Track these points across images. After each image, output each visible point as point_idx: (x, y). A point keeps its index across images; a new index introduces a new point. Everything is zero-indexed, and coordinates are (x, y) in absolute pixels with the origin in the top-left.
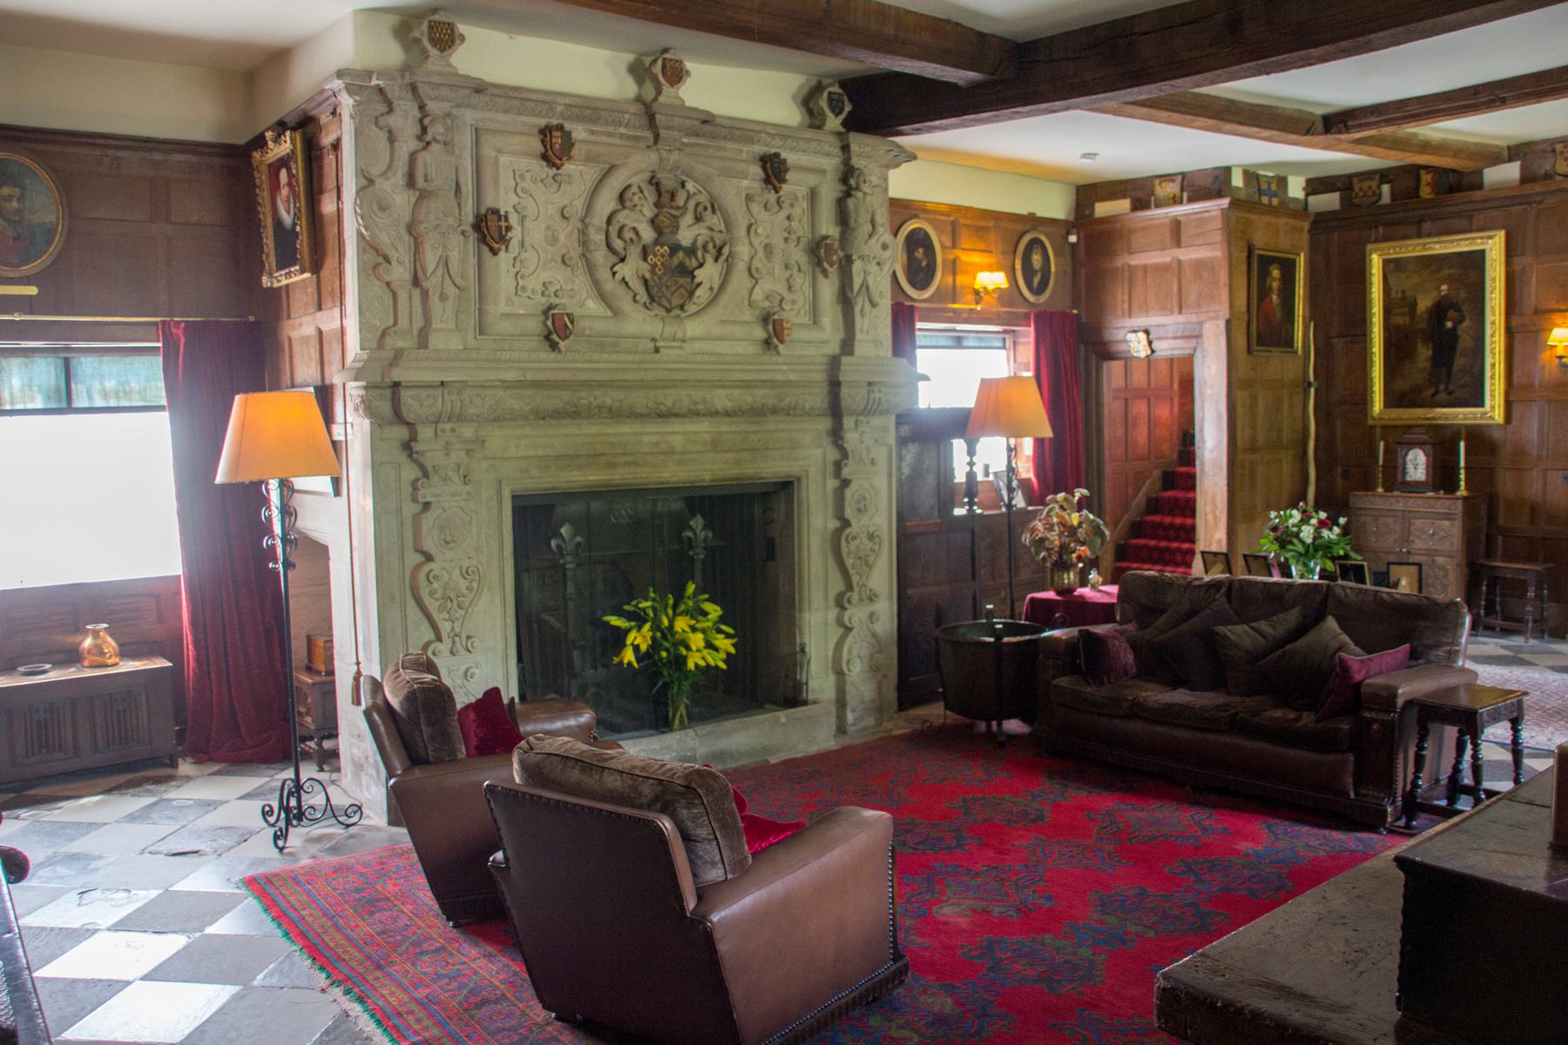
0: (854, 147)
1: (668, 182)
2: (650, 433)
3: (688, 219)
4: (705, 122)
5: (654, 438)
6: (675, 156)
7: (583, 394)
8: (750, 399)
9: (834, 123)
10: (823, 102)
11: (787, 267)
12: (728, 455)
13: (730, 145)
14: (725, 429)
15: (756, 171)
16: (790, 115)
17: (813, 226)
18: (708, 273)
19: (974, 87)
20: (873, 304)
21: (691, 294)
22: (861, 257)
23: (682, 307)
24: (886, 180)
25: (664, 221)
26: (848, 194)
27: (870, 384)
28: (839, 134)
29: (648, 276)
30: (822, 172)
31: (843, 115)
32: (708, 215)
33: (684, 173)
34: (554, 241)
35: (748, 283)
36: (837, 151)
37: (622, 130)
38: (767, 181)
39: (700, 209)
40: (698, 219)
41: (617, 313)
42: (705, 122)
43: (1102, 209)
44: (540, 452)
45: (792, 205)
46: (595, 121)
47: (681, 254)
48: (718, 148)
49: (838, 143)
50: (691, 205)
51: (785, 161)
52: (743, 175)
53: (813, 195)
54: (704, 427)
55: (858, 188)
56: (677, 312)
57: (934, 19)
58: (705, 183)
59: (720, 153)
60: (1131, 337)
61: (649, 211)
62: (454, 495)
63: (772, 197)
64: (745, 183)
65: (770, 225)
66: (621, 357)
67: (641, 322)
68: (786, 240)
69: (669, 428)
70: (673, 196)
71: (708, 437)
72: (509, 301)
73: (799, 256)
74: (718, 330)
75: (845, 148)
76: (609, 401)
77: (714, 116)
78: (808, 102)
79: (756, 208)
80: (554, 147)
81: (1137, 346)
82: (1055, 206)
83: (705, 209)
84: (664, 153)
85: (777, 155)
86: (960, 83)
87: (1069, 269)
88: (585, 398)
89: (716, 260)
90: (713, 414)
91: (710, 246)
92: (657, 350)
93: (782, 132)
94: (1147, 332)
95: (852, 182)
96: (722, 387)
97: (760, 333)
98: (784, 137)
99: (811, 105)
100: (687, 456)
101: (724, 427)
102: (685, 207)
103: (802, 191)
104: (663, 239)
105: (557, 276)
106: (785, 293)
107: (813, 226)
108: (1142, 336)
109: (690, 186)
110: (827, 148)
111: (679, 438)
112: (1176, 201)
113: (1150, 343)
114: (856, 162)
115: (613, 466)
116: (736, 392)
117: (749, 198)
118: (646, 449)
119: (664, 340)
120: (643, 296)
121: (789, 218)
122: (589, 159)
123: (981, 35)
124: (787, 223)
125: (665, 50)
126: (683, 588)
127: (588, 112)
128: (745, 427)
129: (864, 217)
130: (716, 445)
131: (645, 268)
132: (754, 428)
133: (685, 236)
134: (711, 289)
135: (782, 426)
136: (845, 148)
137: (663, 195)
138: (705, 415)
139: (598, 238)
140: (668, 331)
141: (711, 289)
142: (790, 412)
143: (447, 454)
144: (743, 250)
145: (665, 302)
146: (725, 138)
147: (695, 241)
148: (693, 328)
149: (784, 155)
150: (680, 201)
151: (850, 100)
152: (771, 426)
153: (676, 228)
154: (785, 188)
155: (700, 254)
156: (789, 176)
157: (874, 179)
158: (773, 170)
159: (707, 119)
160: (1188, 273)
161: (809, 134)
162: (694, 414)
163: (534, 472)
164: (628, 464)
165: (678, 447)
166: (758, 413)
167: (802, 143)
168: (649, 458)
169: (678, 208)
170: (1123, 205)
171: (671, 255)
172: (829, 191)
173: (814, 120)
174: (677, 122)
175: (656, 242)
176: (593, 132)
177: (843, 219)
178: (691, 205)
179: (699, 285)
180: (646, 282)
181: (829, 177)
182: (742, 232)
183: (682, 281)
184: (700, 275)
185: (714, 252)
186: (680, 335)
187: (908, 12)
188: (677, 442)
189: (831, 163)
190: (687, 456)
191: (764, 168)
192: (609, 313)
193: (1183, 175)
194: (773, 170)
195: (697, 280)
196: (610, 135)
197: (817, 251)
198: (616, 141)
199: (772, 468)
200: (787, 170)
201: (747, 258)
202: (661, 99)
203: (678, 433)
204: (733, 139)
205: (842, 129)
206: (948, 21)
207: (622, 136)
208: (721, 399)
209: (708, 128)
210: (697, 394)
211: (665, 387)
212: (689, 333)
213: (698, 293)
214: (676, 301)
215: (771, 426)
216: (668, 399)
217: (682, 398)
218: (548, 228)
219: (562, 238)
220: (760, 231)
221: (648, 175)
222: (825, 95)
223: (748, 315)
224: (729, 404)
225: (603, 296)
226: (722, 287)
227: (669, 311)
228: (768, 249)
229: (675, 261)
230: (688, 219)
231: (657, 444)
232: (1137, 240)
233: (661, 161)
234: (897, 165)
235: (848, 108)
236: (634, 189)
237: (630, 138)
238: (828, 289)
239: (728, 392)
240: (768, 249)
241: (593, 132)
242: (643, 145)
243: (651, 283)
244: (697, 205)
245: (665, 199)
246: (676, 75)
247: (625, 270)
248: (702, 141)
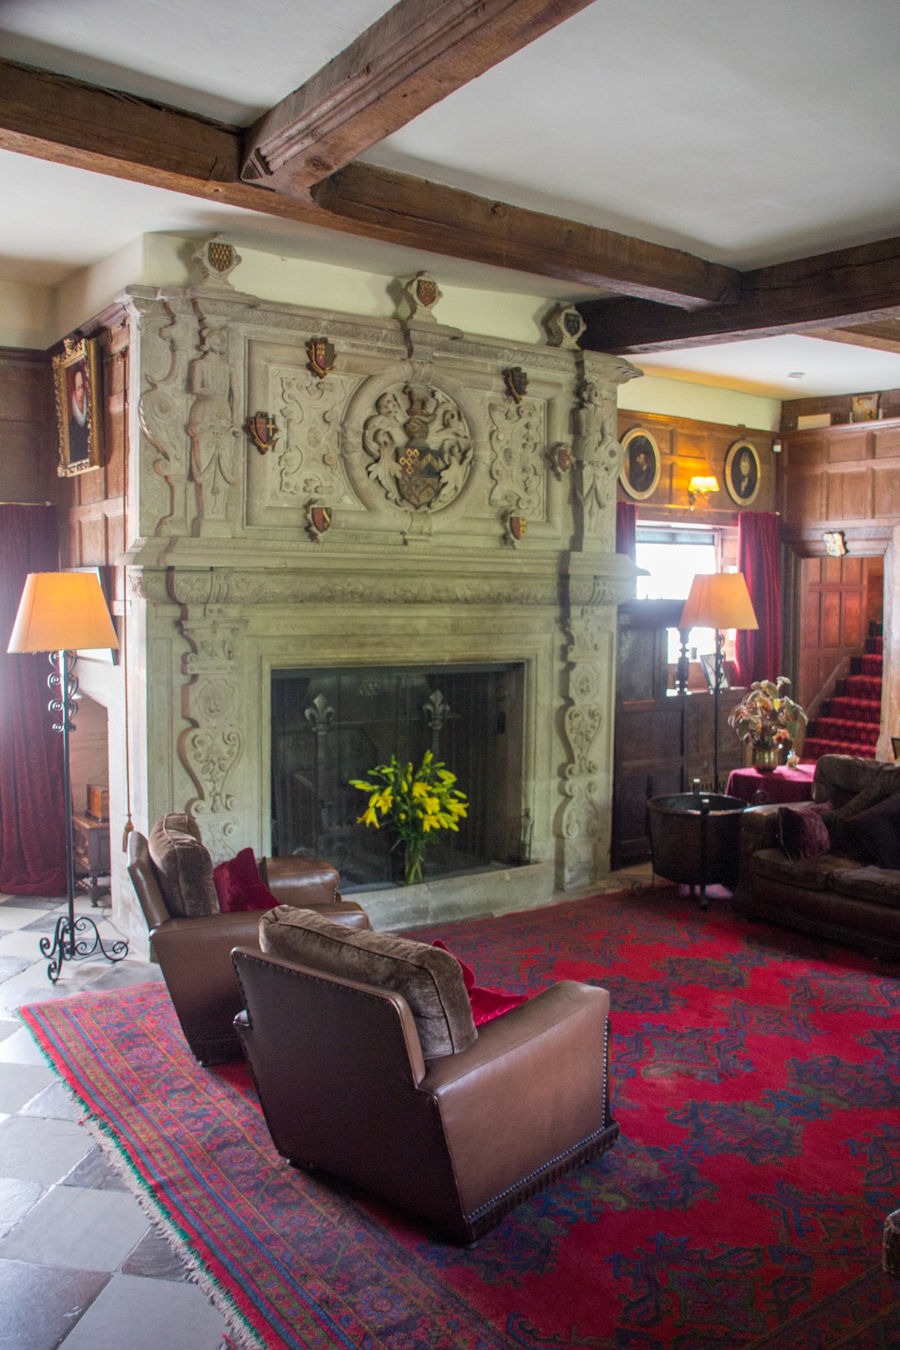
0: (587, 364)
1: (420, 392)
2: (396, 617)
3: (437, 425)
4: (454, 338)
5: (400, 622)
6: (426, 369)
7: (338, 581)
8: (487, 589)
9: (570, 341)
10: (561, 323)
11: (524, 470)
12: (465, 638)
13: (476, 360)
14: (464, 614)
15: (499, 383)
16: (531, 334)
17: (549, 434)
18: (454, 475)
19: (698, 312)
20: (600, 506)
21: (438, 493)
22: (591, 463)
23: (429, 505)
24: (615, 393)
25: (415, 426)
26: (581, 405)
27: (596, 577)
28: (574, 351)
29: (399, 476)
30: (558, 385)
31: (579, 334)
32: (455, 422)
33: (434, 384)
34: (316, 442)
35: (489, 484)
36: (572, 367)
37: (380, 344)
38: (509, 392)
39: (448, 416)
40: (446, 425)
41: (370, 508)
42: (454, 338)
43: (805, 422)
44: (298, 632)
45: (530, 414)
46: (355, 336)
47: (429, 457)
48: (465, 362)
49: (573, 360)
50: (440, 412)
51: (525, 375)
52: (487, 387)
53: (549, 405)
54: (444, 612)
55: (590, 401)
56: (424, 508)
57: (665, 248)
58: (452, 393)
59: (467, 367)
60: (827, 537)
61: (402, 418)
62: (218, 668)
63: (513, 407)
64: (489, 394)
65: (510, 432)
66: (373, 548)
67: (392, 517)
68: (524, 446)
70: (424, 404)
71: (448, 622)
72: (274, 495)
73: (535, 460)
74: (460, 526)
75: (580, 364)
76: (361, 588)
77: (462, 333)
78: (547, 322)
79: (498, 416)
80: (318, 358)
81: (833, 546)
82: (763, 419)
83: (453, 416)
84: (417, 366)
85: (518, 369)
86: (686, 307)
87: (773, 476)
88: (340, 584)
89: (461, 463)
90: (454, 601)
91: (456, 450)
92: (405, 542)
93: (523, 348)
94: (842, 534)
95: (585, 395)
96: (463, 577)
97: (498, 530)
98: (525, 353)
99: (550, 324)
100: (430, 639)
101: (463, 612)
102: (434, 415)
103: (539, 402)
104: (414, 443)
105: (317, 473)
106: (522, 494)
107: (549, 434)
108: (838, 537)
109: (439, 395)
110: (563, 363)
111: (424, 621)
112: (872, 416)
113: (845, 544)
114: (588, 376)
115: (362, 645)
116: (476, 582)
117: (492, 407)
118: (392, 632)
119: (413, 533)
120: (394, 494)
121: (527, 426)
122: (349, 369)
123: (707, 263)
124: (525, 431)
125: (421, 273)
126: (422, 756)
127: (349, 327)
128: (484, 614)
129: (595, 428)
130: (456, 629)
131: (397, 469)
132: (490, 614)
133: (434, 440)
134: (456, 488)
135: (515, 613)
136: (580, 364)
137: (415, 402)
138: (447, 602)
139: (355, 440)
140: (417, 525)
141: (456, 488)
142: (523, 601)
143: (214, 632)
144: (485, 455)
145: (414, 500)
146: (472, 353)
147: (443, 445)
148: (439, 523)
149: (524, 369)
150: (430, 409)
151: (585, 321)
152: (506, 613)
153: (425, 434)
154: (524, 398)
155: (446, 457)
156: (528, 389)
157: (604, 393)
158: (514, 383)
159: (456, 336)
160: (881, 481)
161: (548, 351)
162: (436, 600)
163: (292, 650)
166: (495, 601)
167: (541, 359)
168: (395, 639)
169: (428, 415)
170: (822, 420)
171: (421, 457)
172: (564, 403)
173: (552, 338)
174: (429, 337)
175: (407, 446)
176: (353, 346)
177: (576, 427)
178: (440, 412)
179: (445, 484)
180: (397, 481)
181: (564, 389)
182: (485, 438)
183: (429, 480)
184: (446, 475)
185: (459, 455)
186: (426, 530)
187: (642, 242)
188: (421, 625)
189: (566, 377)
190: (430, 639)
191: (506, 381)
192: (364, 508)
193: (880, 393)
194: (514, 383)
195: (443, 481)
196: (369, 348)
197: (552, 457)
198: (374, 353)
199: (505, 651)
200: (526, 383)
201: (488, 462)
202: (416, 317)
203: (422, 617)
204: (479, 354)
205: (577, 347)
206: (678, 251)
207: (379, 349)
208: (461, 588)
209: (458, 343)
210: (439, 583)
211: (413, 576)
212: (435, 528)
213: (444, 491)
214: (424, 498)
216: (414, 587)
217: (428, 586)
218: (310, 430)
219: (323, 441)
220: (501, 437)
221: (401, 385)
222: (563, 316)
223: (488, 513)
224: (469, 593)
225: (358, 493)
226: (466, 487)
227: (417, 508)
228: (508, 454)
229: (424, 463)
230: (437, 425)
231: (403, 627)
232: (836, 451)
233: (414, 372)
234: (625, 381)
235: (583, 328)
236: (389, 397)
237: (386, 351)
238: (561, 490)
239: (469, 581)
240: (508, 454)
241: (353, 346)
242: (398, 358)
243: (402, 482)
244: (446, 412)
245: (417, 407)
246: (430, 295)
247: (379, 470)
248: (451, 356)
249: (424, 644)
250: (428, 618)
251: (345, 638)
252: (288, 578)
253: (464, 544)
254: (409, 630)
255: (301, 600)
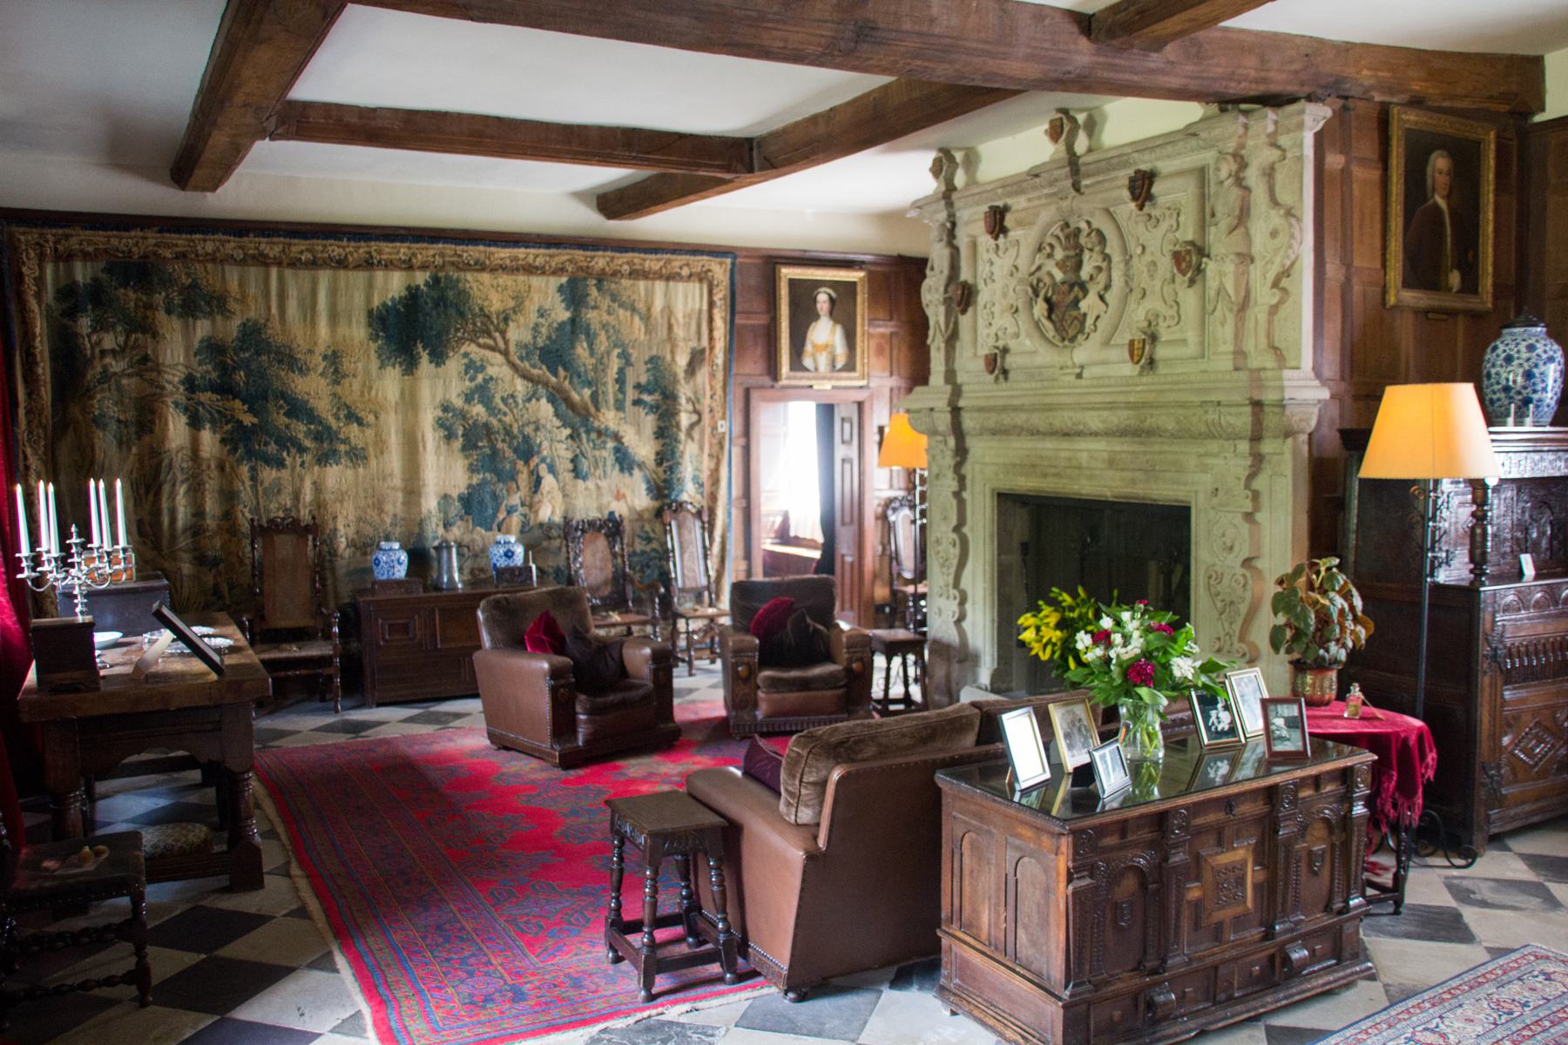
5: (1067, 454)
12: (1126, 474)
14: (1118, 448)
37: (1046, 191)
44: (1001, 460)
54: (1099, 445)
66: (1039, 385)
67: (1046, 356)
69: (1077, 446)
71: (1105, 455)
85: (1137, 172)
88: (1008, 419)
90: (1095, 434)
96: (1093, 409)
97: (1161, 352)
115: (1045, 475)
116: (1105, 414)
126: (1111, 593)
128: (1136, 448)
130: (1112, 463)
132: (1142, 448)
135: (1166, 448)
152: (1157, 448)
164: (1055, 475)
165: (1084, 464)
168: (1069, 471)
196: (1039, 198)
198: (1044, 201)
199: (1163, 491)
208: (1094, 421)
210: (1078, 416)
214: (1071, 333)
215: (1157, 448)
231: (1070, 459)
248: (1100, 178)
249: (1091, 477)
250: (1089, 451)
251: (1031, 468)
252: (976, 415)
253: (1112, 373)
254: (1075, 463)
255: (994, 432)
